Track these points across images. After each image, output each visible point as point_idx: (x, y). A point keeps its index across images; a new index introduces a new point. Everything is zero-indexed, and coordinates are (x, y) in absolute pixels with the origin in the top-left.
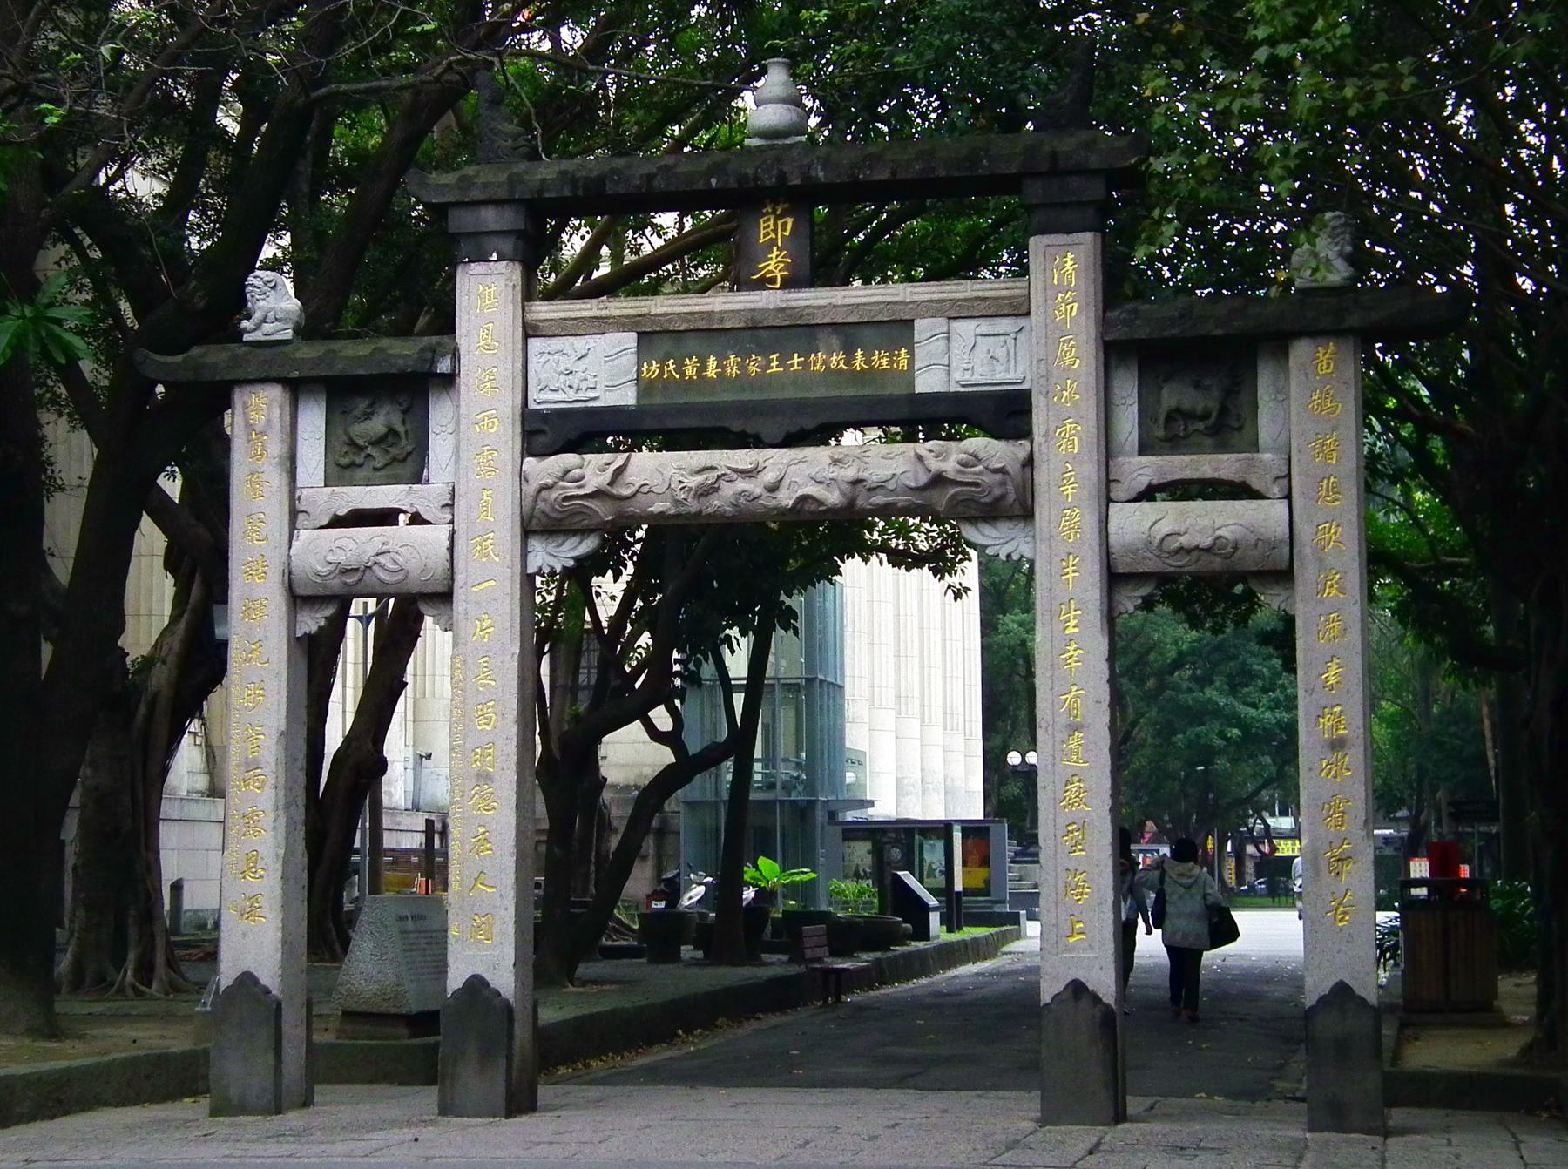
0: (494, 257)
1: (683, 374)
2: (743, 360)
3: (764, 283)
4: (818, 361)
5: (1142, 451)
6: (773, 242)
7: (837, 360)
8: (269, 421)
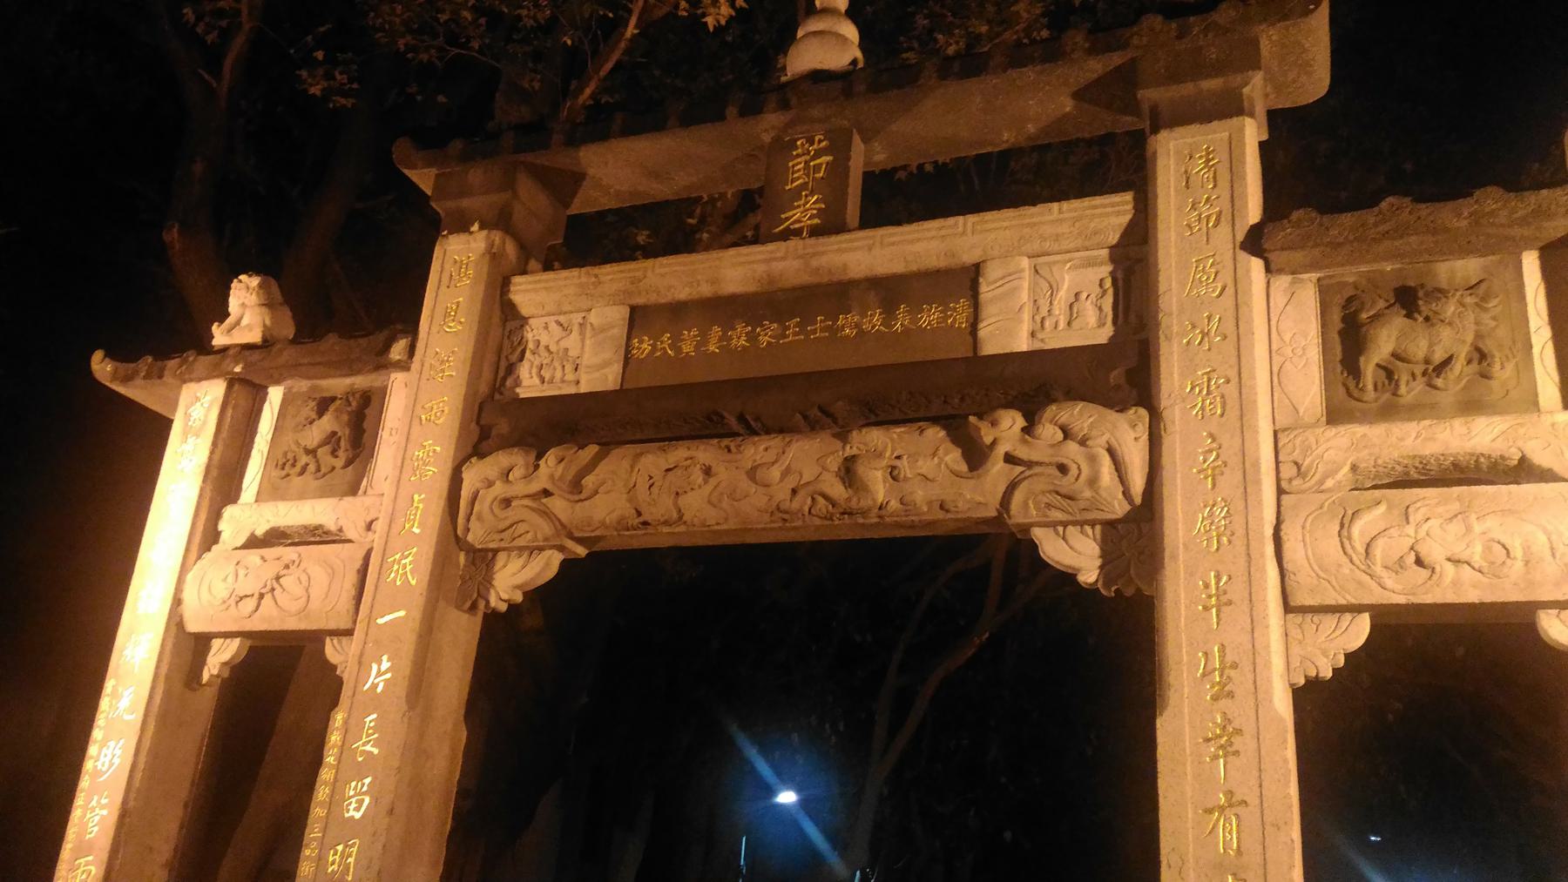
0: (475, 227)
1: (678, 350)
2: (754, 330)
3: (787, 235)
4: (847, 324)
5: (1335, 415)
6: (804, 186)
7: (874, 321)
8: (205, 423)
